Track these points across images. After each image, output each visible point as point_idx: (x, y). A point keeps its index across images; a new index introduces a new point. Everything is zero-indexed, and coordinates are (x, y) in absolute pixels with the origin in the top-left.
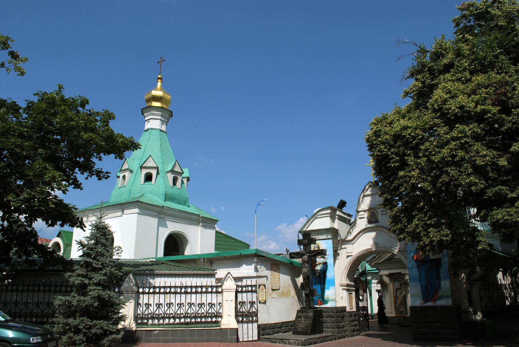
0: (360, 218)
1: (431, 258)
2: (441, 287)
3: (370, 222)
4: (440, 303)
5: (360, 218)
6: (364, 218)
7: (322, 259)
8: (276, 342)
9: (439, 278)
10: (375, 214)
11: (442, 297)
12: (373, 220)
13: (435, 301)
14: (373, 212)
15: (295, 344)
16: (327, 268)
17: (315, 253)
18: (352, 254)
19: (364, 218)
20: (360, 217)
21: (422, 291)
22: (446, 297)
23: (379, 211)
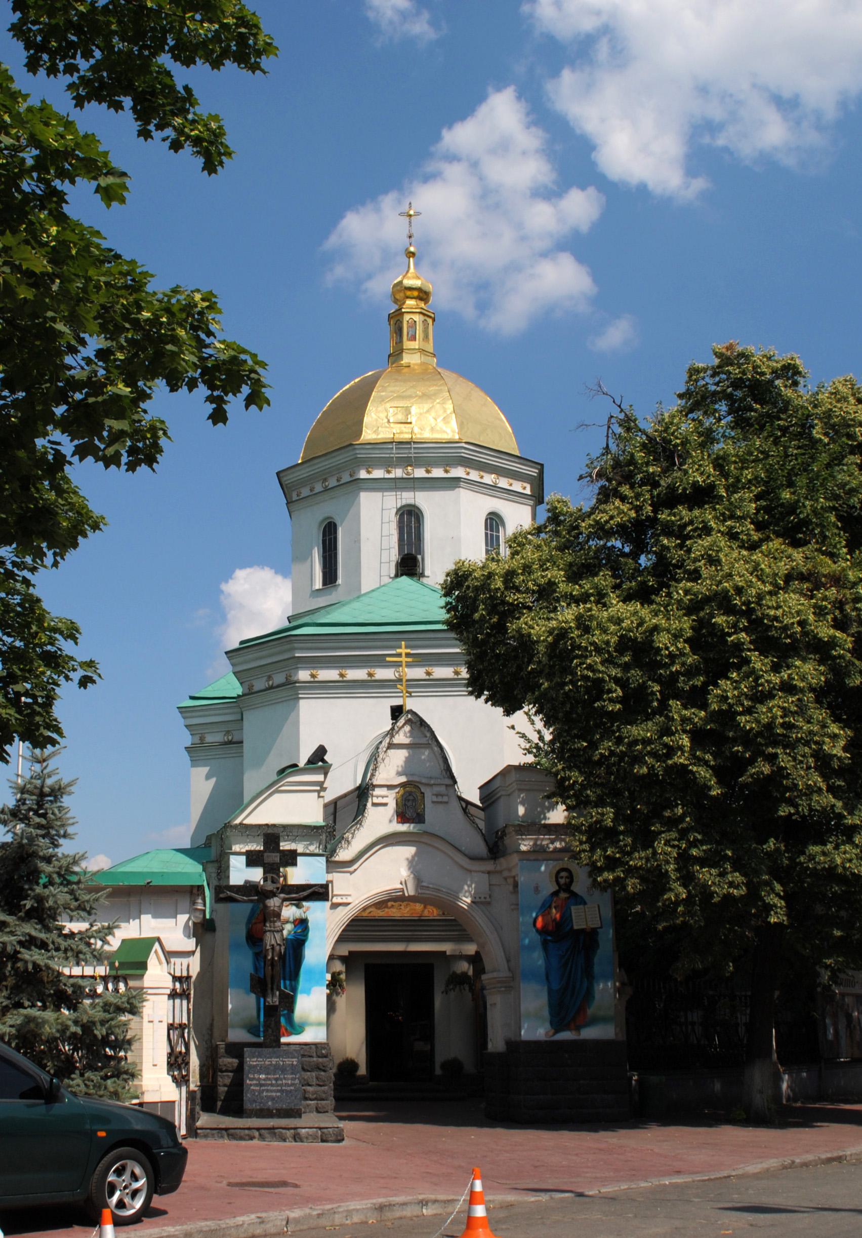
0: (374, 805)
1: (575, 927)
2: (594, 997)
3: (402, 816)
4: (590, 1033)
5: (374, 805)
6: (385, 805)
7: (294, 908)
8: (252, 1138)
9: (589, 975)
10: (414, 800)
11: (594, 1021)
12: (409, 814)
13: (578, 1029)
14: (410, 793)
15: (314, 1138)
16: (306, 936)
17: (305, 893)
18: (349, 900)
19: (385, 805)
20: (375, 800)
21: (551, 1006)
22: (604, 1020)
23: (428, 792)
